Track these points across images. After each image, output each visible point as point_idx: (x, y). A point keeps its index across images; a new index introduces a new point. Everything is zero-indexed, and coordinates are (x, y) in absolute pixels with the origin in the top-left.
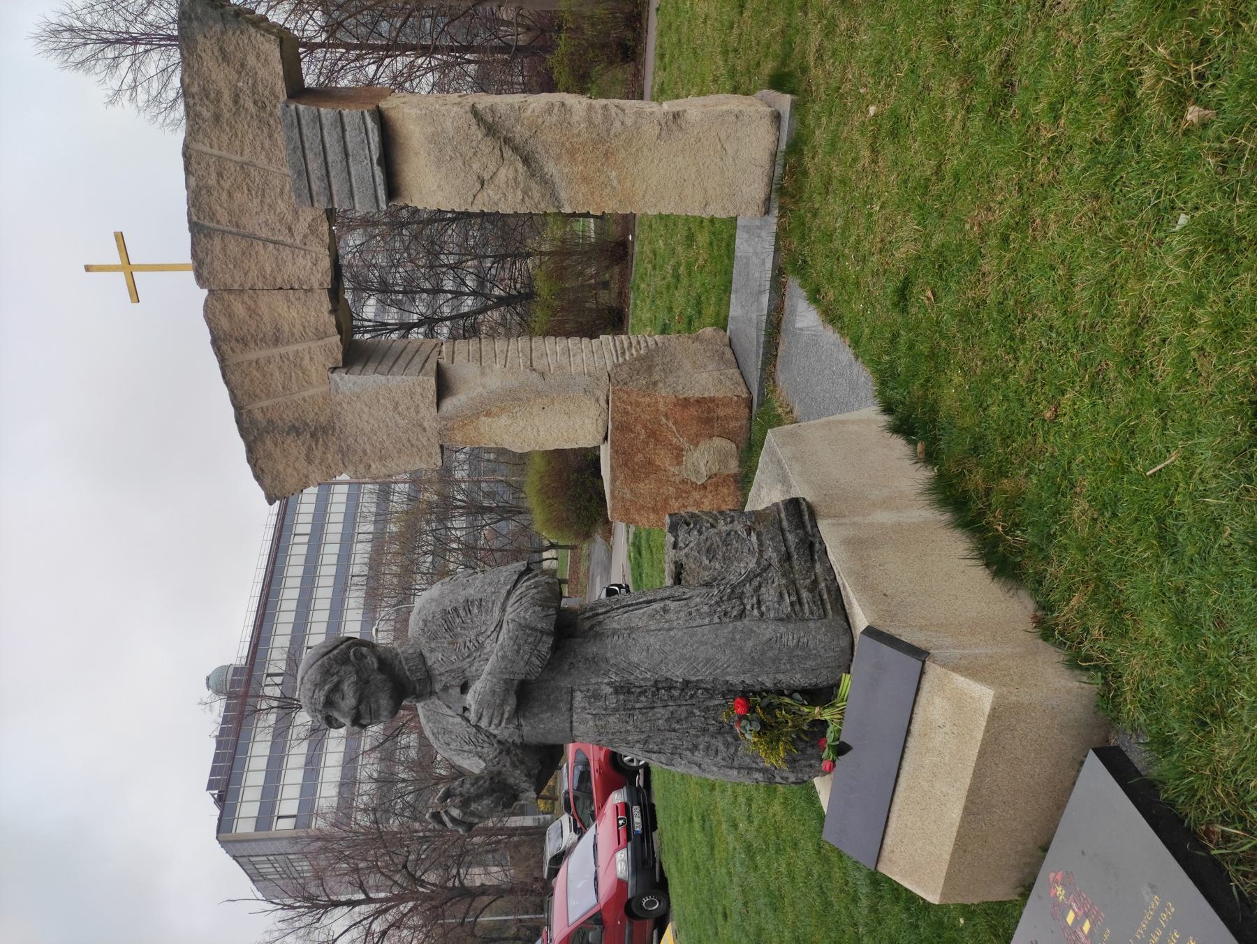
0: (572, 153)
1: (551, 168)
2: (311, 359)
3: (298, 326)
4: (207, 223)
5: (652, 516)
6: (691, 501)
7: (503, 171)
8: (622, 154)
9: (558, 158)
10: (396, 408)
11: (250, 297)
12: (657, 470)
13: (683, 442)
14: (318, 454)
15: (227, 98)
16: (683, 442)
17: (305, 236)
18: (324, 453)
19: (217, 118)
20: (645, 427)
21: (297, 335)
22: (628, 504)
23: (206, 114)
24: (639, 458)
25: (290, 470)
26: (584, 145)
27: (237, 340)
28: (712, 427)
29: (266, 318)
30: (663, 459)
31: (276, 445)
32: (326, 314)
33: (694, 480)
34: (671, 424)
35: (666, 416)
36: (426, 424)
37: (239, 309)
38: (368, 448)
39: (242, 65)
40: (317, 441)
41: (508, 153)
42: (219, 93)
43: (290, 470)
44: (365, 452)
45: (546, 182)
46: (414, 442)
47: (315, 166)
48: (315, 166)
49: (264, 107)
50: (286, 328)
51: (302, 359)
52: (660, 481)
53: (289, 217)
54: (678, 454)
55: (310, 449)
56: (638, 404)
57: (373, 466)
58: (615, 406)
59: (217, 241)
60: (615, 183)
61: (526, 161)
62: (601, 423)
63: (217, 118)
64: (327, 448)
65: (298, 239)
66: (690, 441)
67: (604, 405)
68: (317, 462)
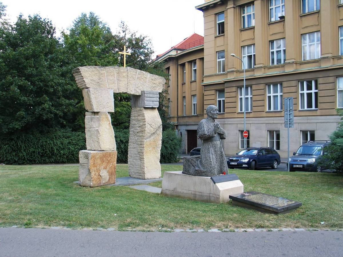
0: (155, 141)
1: (152, 137)
2: (115, 86)
3: (121, 85)
4: (138, 73)
5: (92, 163)
6: (96, 173)
7: (153, 129)
8: (154, 150)
9: (154, 139)
10: (108, 103)
11: (126, 77)
12: (102, 163)
13: (108, 169)
14: (93, 82)
15: (155, 82)
16: (108, 169)
17: (136, 90)
18: (93, 84)
19: (152, 80)
20: (110, 160)
21: (119, 84)
22: (95, 157)
23: (153, 78)
24: (104, 159)
25: (89, 75)
26: (156, 143)
27: (119, 72)
28: (111, 175)
29: (122, 79)
30: (104, 164)
31: (96, 74)
32: (123, 91)
33: (101, 173)
34: (111, 165)
35: (112, 164)
36: (104, 109)
37: (124, 74)
38: (98, 95)
39: (158, 86)
40: (97, 83)
41: (156, 130)
42: (155, 81)
43: (89, 75)
44: (96, 94)
45: (150, 136)
46: (100, 106)
47: (151, 95)
48: (151, 95)
49: (153, 88)
50: (121, 82)
51: (115, 84)
52: (100, 164)
53: (139, 88)
54: (105, 168)
55: (94, 81)
56: (114, 158)
57: (93, 95)
58: (113, 152)
59: (135, 74)
60: (149, 149)
61: (154, 133)
62: (108, 149)
63: (152, 80)
64: (95, 85)
65: (136, 89)
66: (108, 170)
67: (112, 150)
68: (91, 82)
